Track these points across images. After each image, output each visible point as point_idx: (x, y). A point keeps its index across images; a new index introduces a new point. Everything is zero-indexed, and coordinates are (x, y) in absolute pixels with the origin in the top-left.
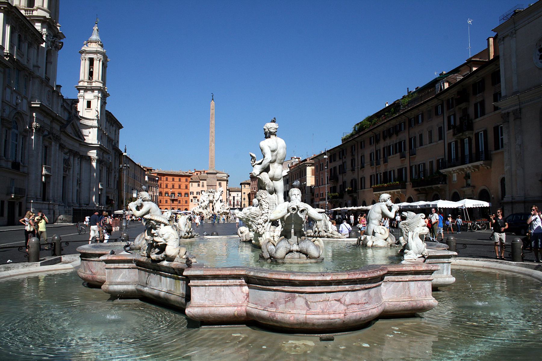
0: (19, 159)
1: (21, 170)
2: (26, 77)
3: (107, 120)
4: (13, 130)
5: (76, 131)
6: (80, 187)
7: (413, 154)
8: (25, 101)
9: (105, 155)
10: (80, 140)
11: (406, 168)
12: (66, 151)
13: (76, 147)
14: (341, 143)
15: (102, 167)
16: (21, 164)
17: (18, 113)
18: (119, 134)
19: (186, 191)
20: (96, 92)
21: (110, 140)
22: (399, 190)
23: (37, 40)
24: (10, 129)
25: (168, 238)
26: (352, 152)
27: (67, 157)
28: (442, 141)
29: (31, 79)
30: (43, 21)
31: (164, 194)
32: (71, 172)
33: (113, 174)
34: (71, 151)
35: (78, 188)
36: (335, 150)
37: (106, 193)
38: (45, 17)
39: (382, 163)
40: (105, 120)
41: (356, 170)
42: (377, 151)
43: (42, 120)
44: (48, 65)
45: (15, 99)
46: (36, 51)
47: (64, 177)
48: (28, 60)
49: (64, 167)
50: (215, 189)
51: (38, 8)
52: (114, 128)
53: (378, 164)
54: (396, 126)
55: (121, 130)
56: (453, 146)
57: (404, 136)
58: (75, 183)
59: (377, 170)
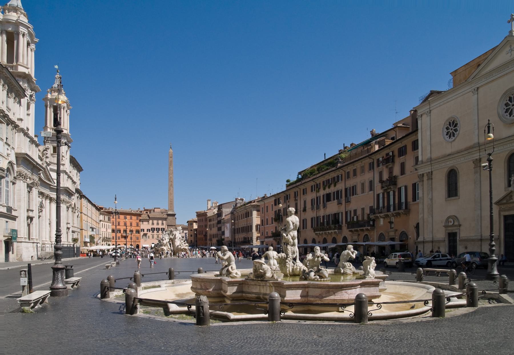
7: (348, 201)
11: (342, 213)
14: (284, 189)
19: (138, 228)
22: (336, 231)
26: (295, 197)
28: (372, 192)
36: (280, 195)
39: (322, 207)
41: (299, 213)
42: (317, 198)
53: (318, 208)
54: (334, 178)
56: (381, 196)
57: (341, 186)
59: (318, 213)
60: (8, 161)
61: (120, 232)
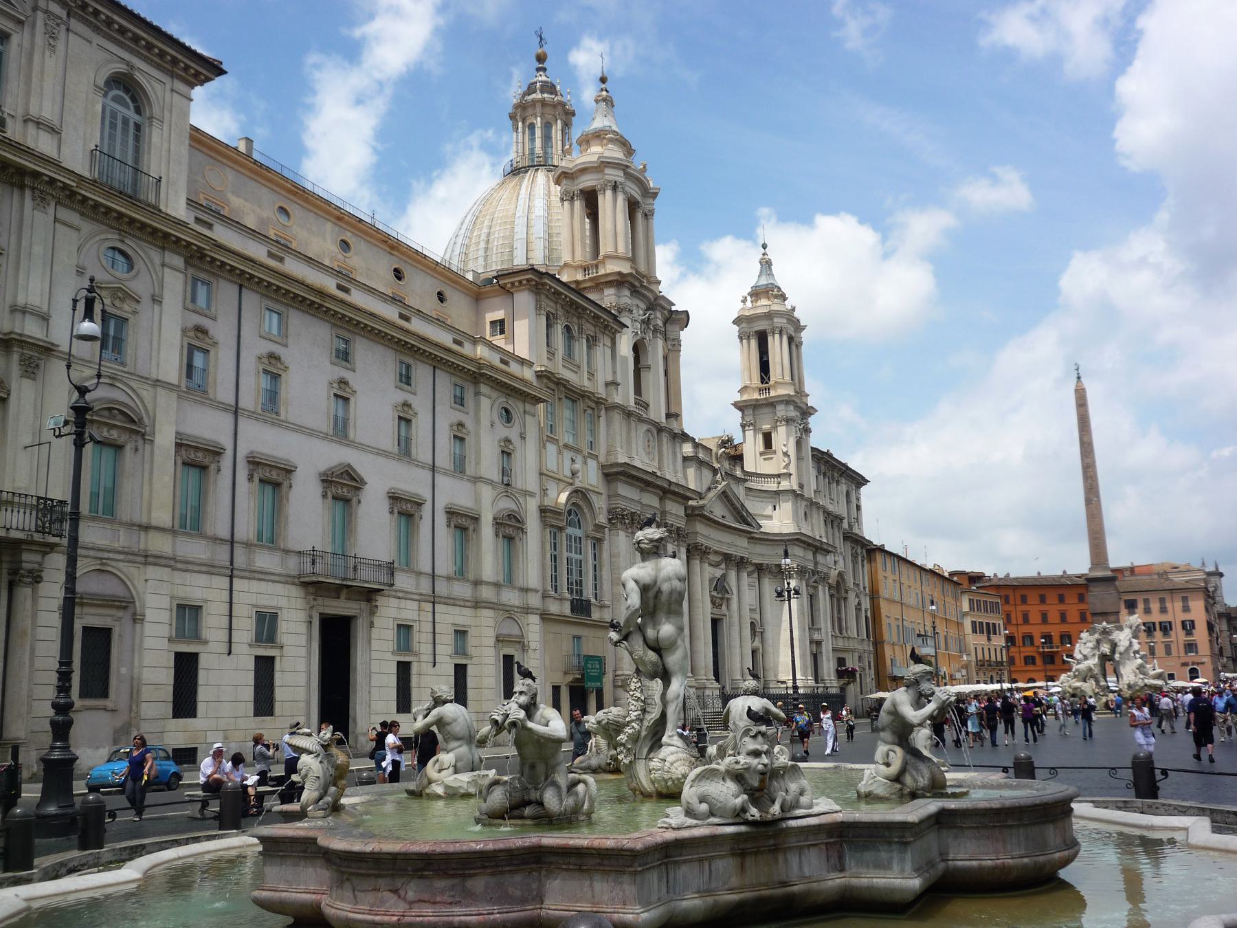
0: (588, 593)
1: (596, 615)
2: (590, 411)
3: (819, 471)
4: (570, 530)
5: (736, 509)
6: (762, 641)
8: (592, 464)
9: (820, 558)
10: (748, 528)
12: (713, 558)
13: (740, 546)
15: (815, 588)
16: (593, 600)
17: (576, 491)
18: (858, 499)
20: (781, 411)
21: (832, 520)
23: (606, 327)
24: (561, 529)
25: (306, 776)
27: (718, 573)
29: (603, 413)
30: (620, 281)
31: (1019, 641)
32: (734, 605)
33: (852, 601)
34: (727, 558)
35: (757, 643)
37: (835, 650)
38: (619, 273)
40: (813, 472)
43: (636, 498)
44: (643, 374)
45: (567, 463)
46: (608, 351)
47: (715, 623)
48: (591, 375)
49: (712, 597)
50: (1118, 621)
51: (606, 257)
52: (843, 488)
55: (863, 489)
58: (747, 632)
60: (570, 489)
61: (1032, 644)
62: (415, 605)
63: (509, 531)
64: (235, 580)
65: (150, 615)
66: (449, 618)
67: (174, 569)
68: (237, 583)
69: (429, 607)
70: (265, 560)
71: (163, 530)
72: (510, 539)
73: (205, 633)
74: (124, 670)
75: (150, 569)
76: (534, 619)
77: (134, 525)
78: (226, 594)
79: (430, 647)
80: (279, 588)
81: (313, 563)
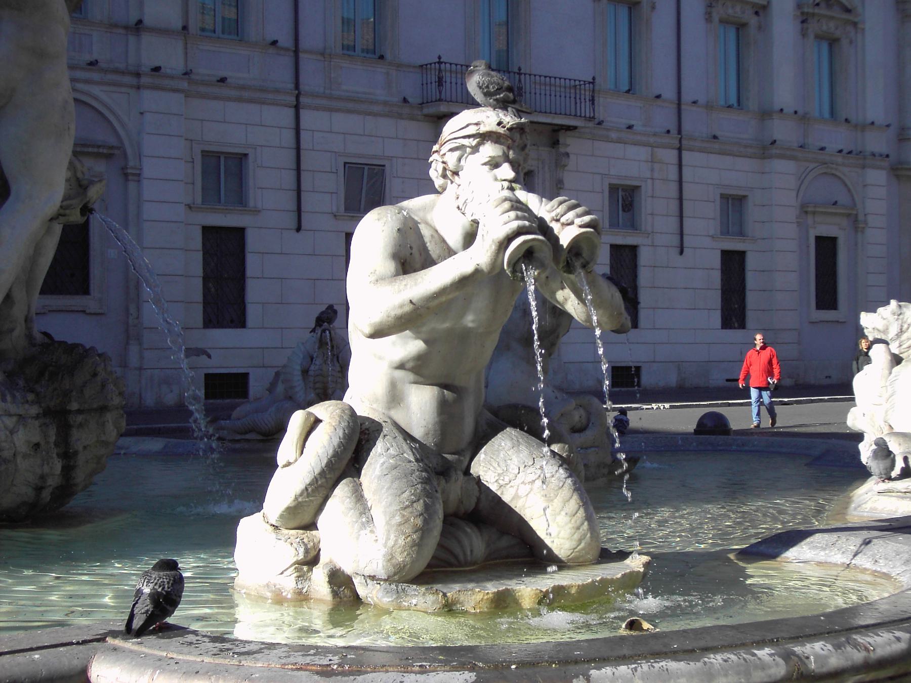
62: (643, 153)
63: (829, 27)
64: (303, 113)
65: (150, 169)
66: (708, 174)
67: (188, 95)
68: (307, 117)
69: (670, 156)
70: (358, 78)
71: (163, 32)
72: (833, 42)
73: (255, 198)
74: (112, 253)
75: (147, 94)
76: (877, 177)
77: (116, 26)
78: (289, 135)
79: (673, 222)
80: (386, 126)
81: (440, 82)
